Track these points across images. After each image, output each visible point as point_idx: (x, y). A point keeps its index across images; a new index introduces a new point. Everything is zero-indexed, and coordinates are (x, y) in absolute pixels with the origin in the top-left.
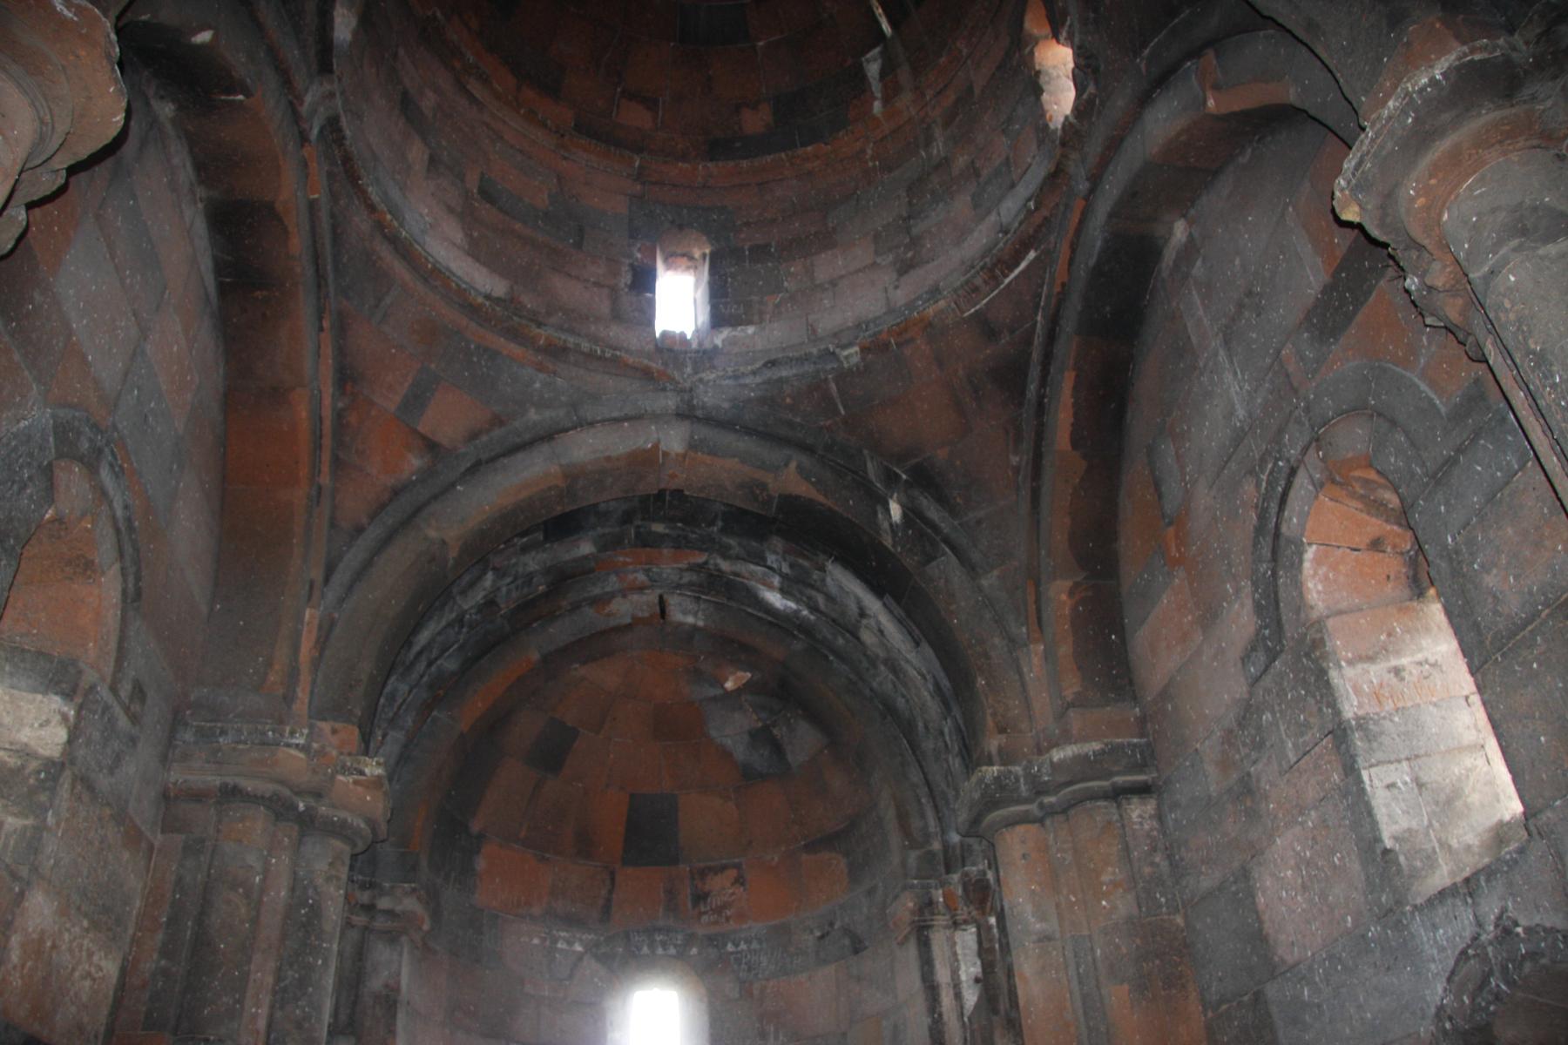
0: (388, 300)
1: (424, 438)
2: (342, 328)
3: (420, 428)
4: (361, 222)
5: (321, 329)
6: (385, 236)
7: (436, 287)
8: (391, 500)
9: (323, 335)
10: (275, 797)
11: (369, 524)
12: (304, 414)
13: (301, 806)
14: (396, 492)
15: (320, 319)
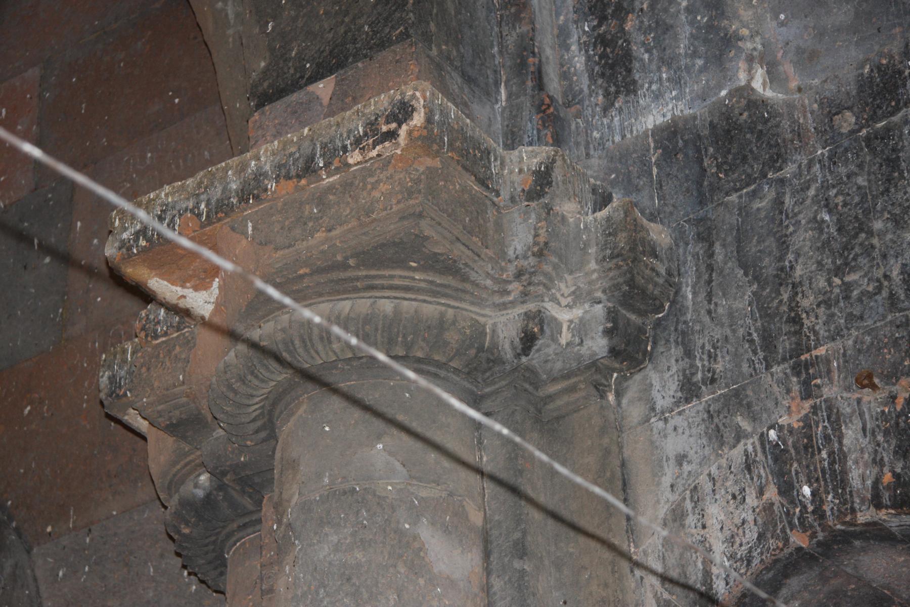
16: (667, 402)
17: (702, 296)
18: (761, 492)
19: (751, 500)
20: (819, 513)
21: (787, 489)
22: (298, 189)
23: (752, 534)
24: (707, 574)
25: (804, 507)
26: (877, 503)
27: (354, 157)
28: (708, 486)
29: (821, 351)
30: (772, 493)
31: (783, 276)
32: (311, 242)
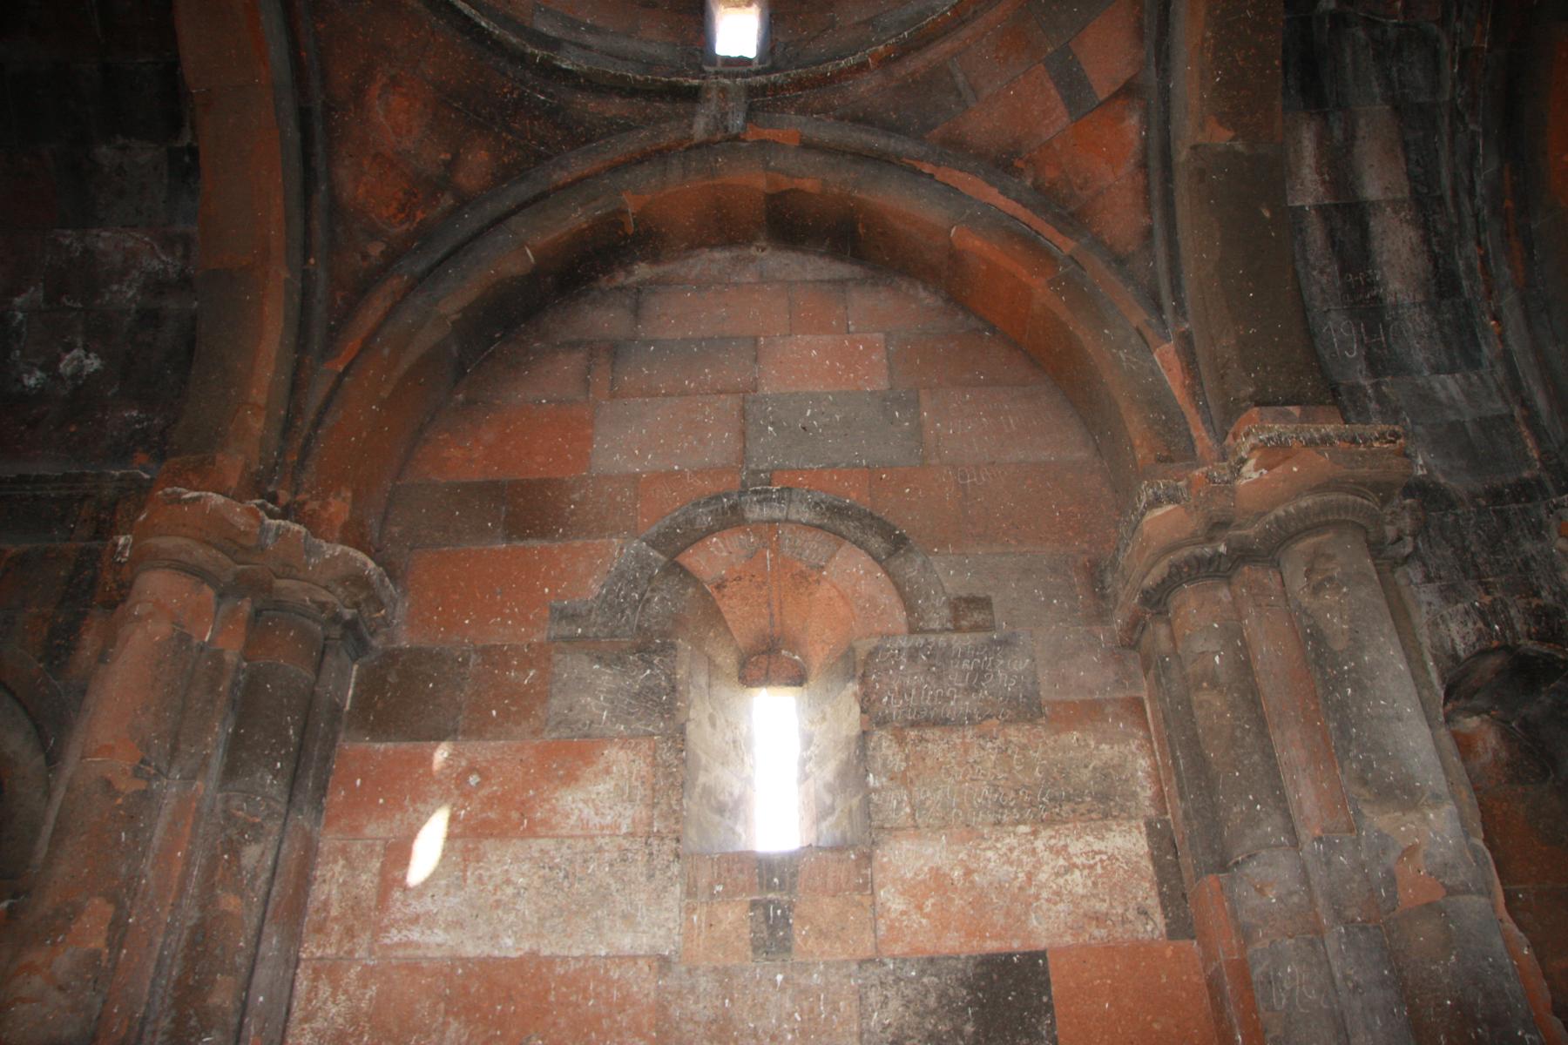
0: (960, 78)
1: (1115, 96)
2: (956, 148)
3: (1102, 96)
4: (866, 88)
5: (931, 176)
6: (897, 59)
7: (975, 12)
8: (1147, 176)
9: (938, 177)
10: (1174, 570)
11: (1151, 218)
12: (978, 243)
13: (1222, 549)
14: (1143, 165)
15: (922, 174)
16: (1419, 581)
17: (1427, 546)
18: (1475, 623)
19: (1470, 625)
20: (1504, 635)
21: (1488, 625)
22: (1349, 448)
23: (1473, 638)
24: (1454, 649)
25: (1497, 634)
26: (1529, 636)
27: (1376, 444)
28: (1448, 617)
29: (1491, 579)
30: (1480, 625)
31: (1465, 549)
32: (1361, 470)
